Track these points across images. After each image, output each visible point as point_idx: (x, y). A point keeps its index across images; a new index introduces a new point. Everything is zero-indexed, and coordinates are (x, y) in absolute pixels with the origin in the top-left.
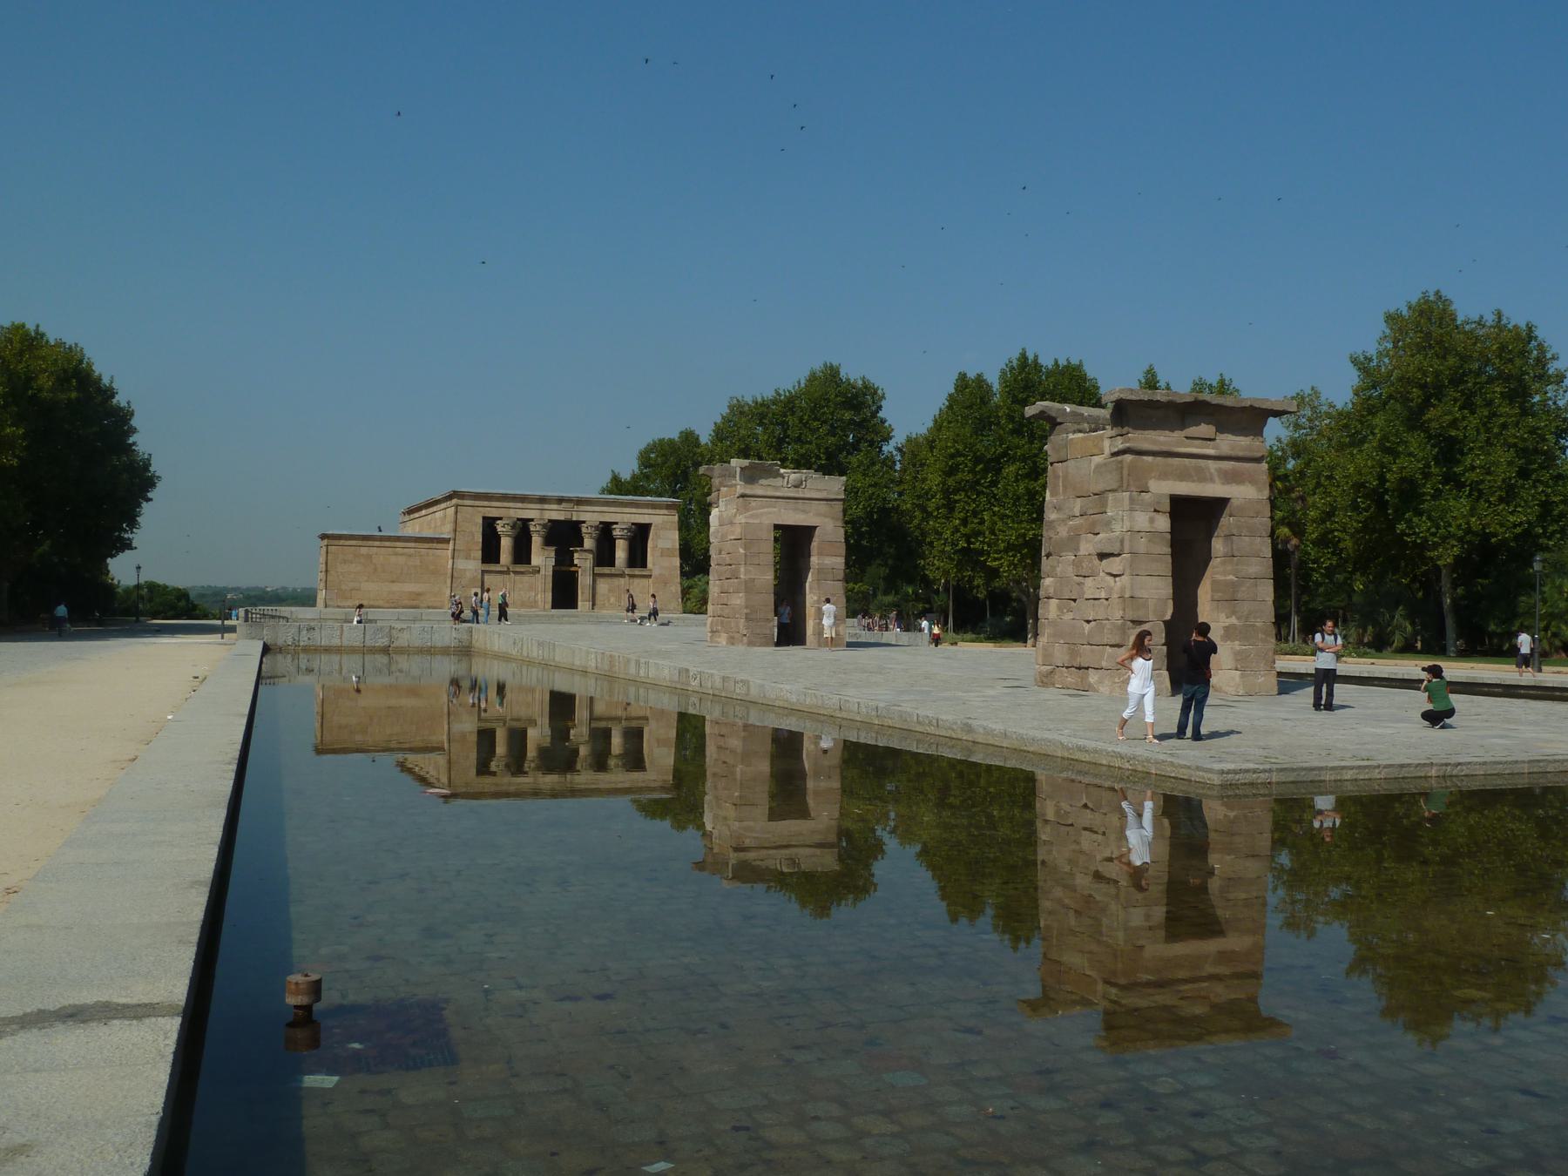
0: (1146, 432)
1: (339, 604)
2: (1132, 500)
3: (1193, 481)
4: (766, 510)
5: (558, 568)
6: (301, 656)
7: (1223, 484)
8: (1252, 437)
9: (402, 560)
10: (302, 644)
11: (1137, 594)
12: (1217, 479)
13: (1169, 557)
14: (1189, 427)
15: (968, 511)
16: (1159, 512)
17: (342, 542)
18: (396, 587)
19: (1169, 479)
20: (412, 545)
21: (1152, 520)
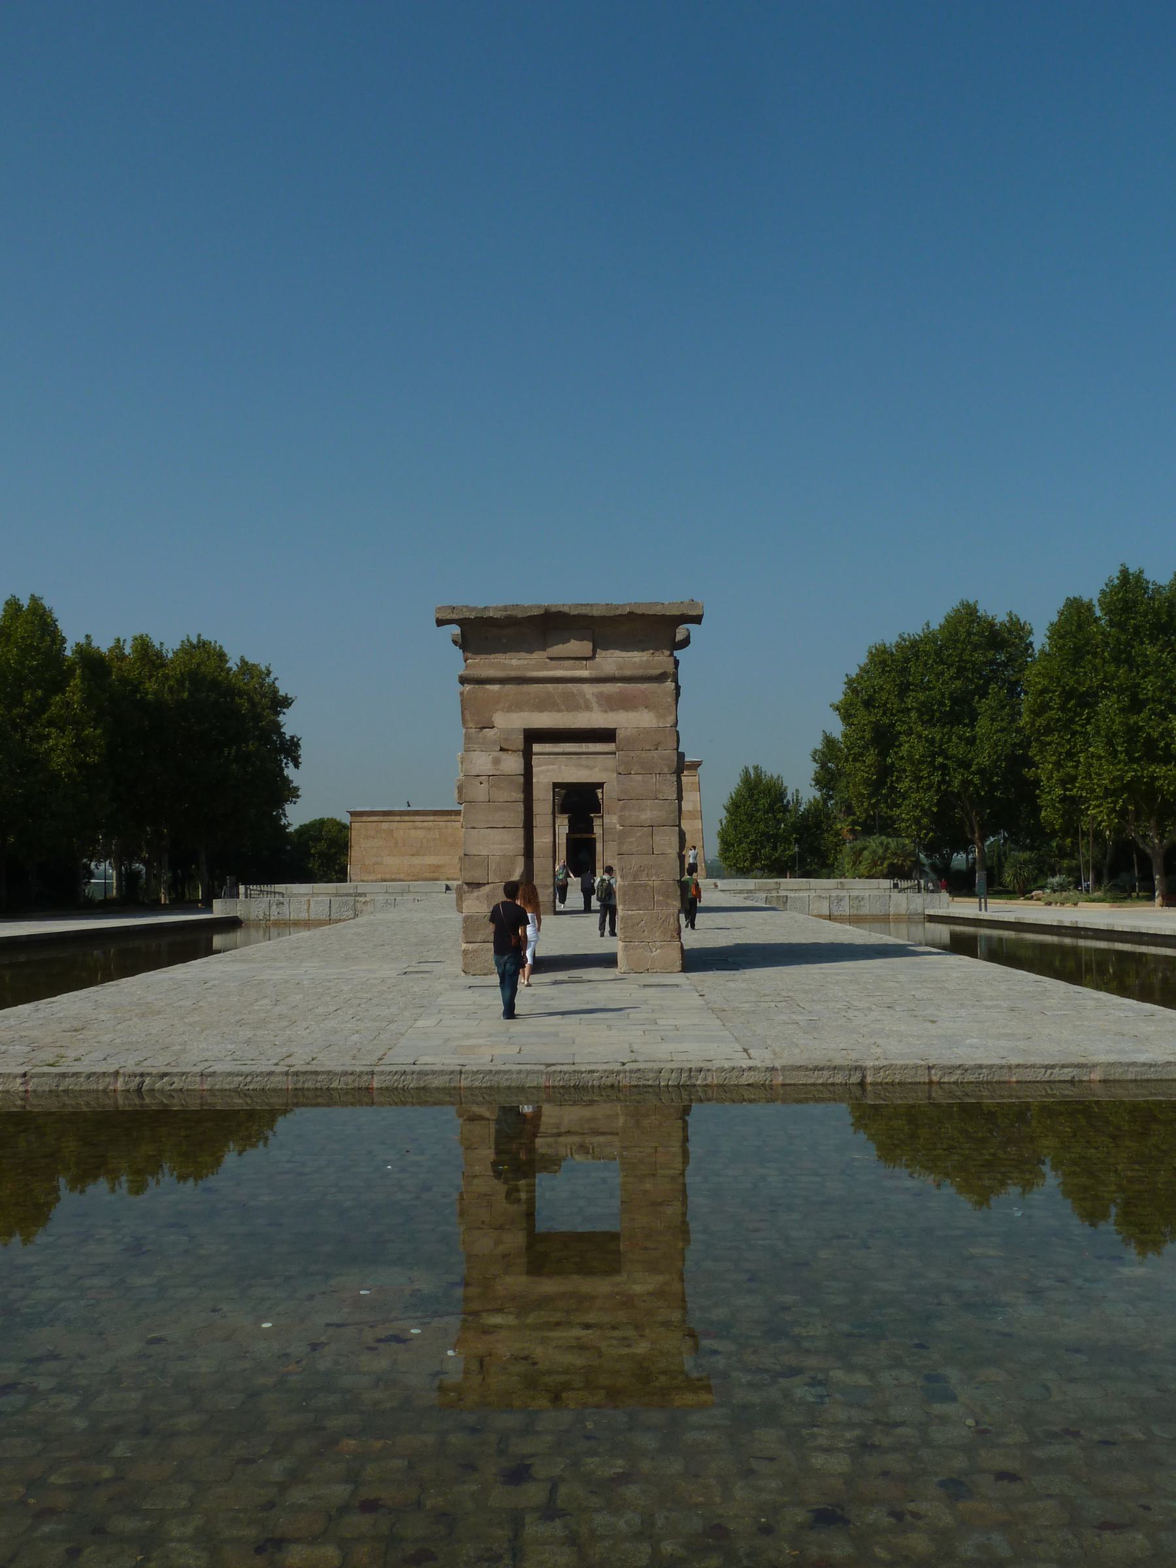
0: (492, 656)
1: (363, 878)
2: (468, 738)
3: (559, 711)
4: (544, 767)
5: (578, 836)
6: (272, 930)
7: (606, 711)
8: (651, 651)
9: (420, 834)
10: (272, 918)
11: (473, 851)
12: (595, 705)
13: (522, 805)
14: (552, 646)
15: (1060, 754)
16: (507, 750)
17: (364, 819)
18: (417, 861)
19: (522, 710)
20: (432, 818)
21: (496, 761)
